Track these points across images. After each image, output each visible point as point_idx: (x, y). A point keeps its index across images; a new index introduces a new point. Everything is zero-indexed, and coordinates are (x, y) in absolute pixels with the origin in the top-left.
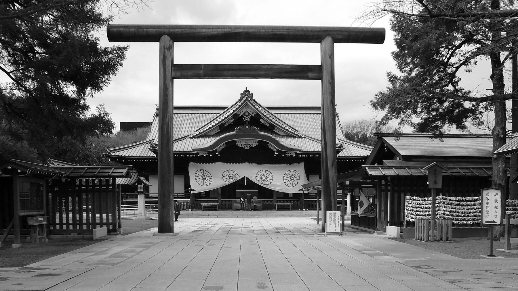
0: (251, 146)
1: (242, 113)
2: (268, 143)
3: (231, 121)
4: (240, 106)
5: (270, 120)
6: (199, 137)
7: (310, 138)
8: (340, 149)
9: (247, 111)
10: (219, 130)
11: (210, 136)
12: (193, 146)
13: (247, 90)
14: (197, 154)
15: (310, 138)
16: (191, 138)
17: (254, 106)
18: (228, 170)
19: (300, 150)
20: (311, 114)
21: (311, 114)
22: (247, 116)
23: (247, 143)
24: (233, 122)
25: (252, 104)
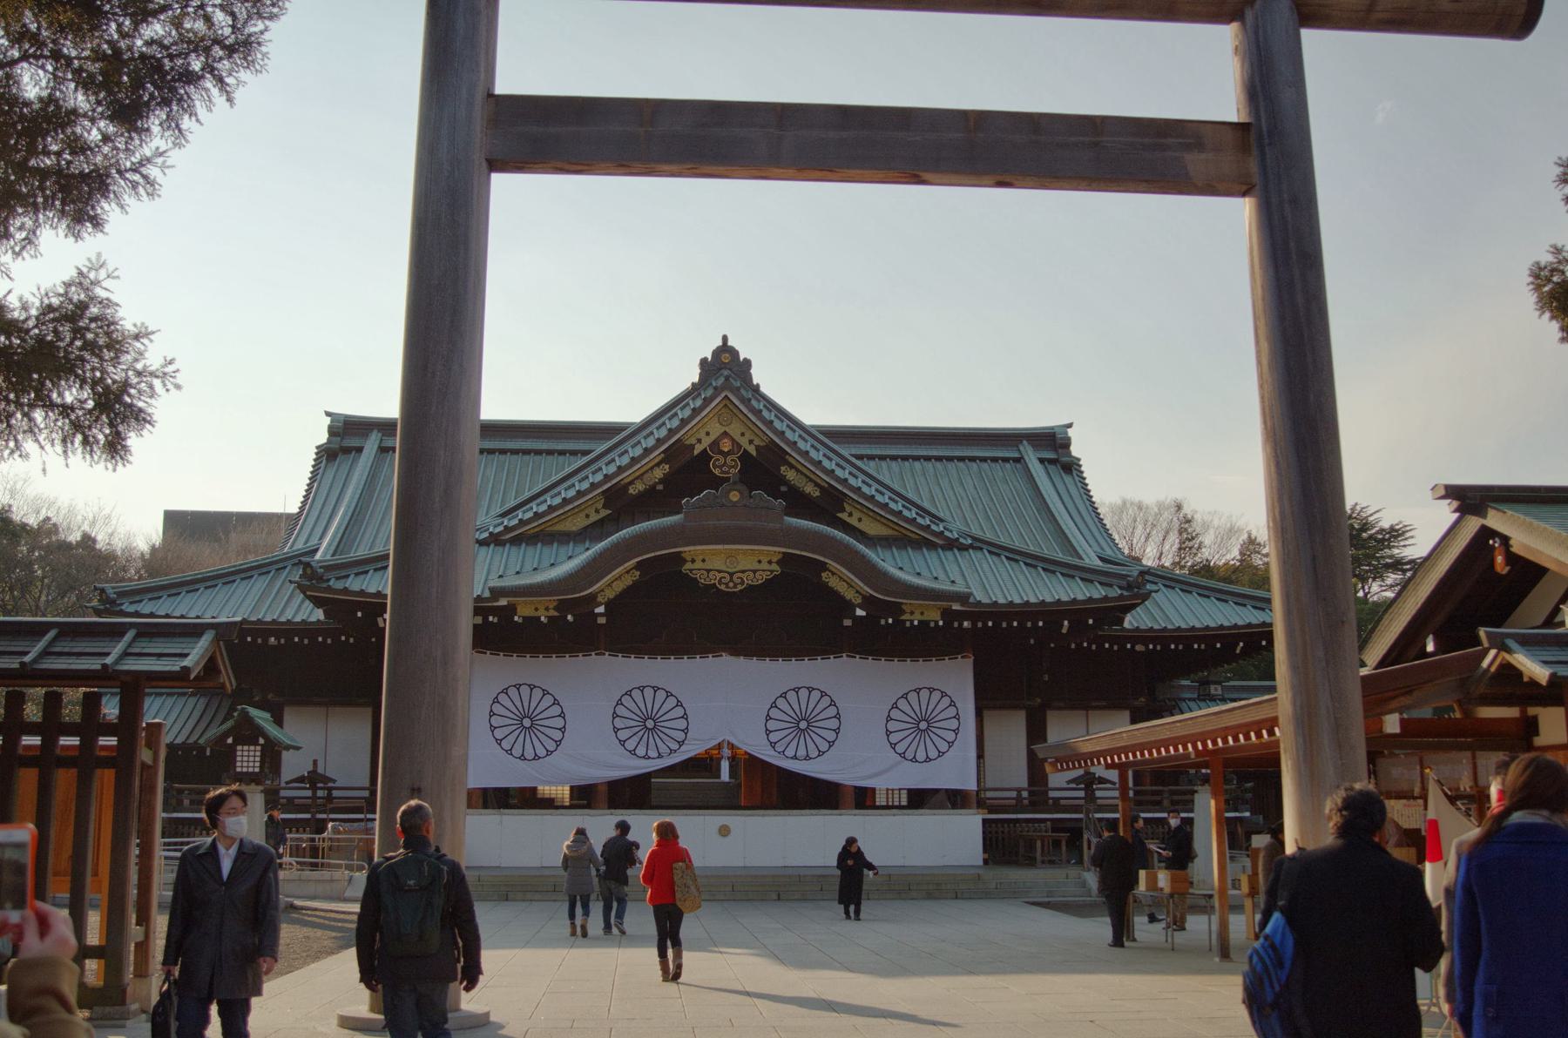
0: (749, 580)
1: (706, 442)
2: (823, 567)
3: (658, 474)
4: (696, 412)
5: (825, 470)
6: (516, 541)
7: (996, 549)
8: (1136, 596)
11: (565, 538)
12: (494, 575)
14: (512, 609)
15: (996, 549)
17: (758, 413)
19: (963, 598)
20: (973, 459)
21: (973, 459)
23: (732, 563)
24: (665, 480)
25: (747, 402)
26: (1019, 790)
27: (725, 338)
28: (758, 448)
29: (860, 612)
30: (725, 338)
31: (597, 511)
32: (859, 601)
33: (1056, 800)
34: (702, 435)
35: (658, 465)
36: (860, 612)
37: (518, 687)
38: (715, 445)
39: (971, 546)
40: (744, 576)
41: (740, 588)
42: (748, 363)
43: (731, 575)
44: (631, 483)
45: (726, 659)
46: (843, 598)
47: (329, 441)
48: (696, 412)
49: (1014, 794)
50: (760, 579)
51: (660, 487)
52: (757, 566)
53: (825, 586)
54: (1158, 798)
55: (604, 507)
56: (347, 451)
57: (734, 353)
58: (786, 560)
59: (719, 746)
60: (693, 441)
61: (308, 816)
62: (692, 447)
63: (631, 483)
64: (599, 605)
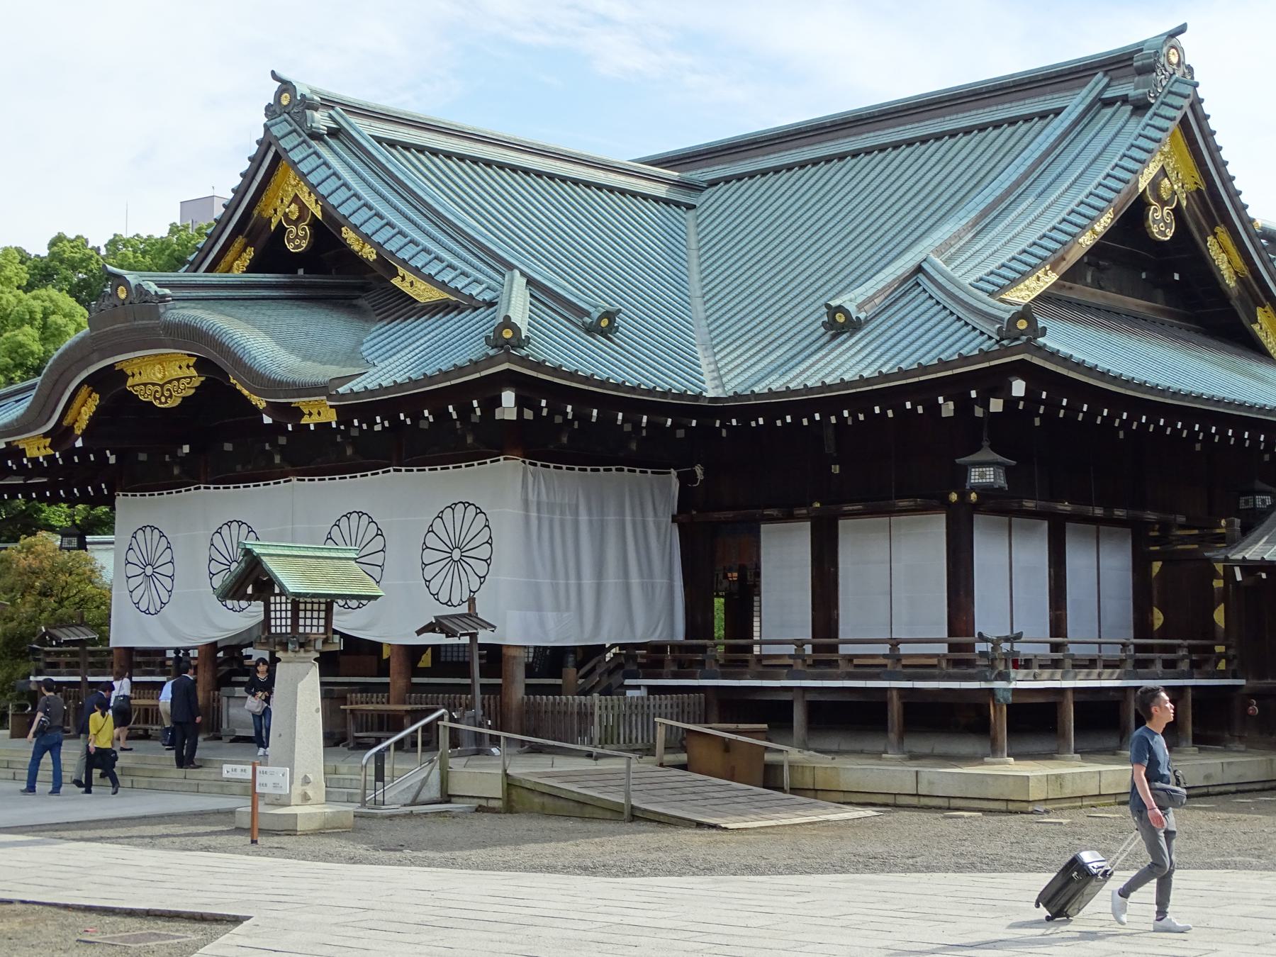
22: (296, 223)
26: (800, 644)
27: (274, 75)
33: (850, 658)
40: (169, 386)
43: (162, 386)
49: (791, 649)
52: (180, 374)
61: (78, 679)
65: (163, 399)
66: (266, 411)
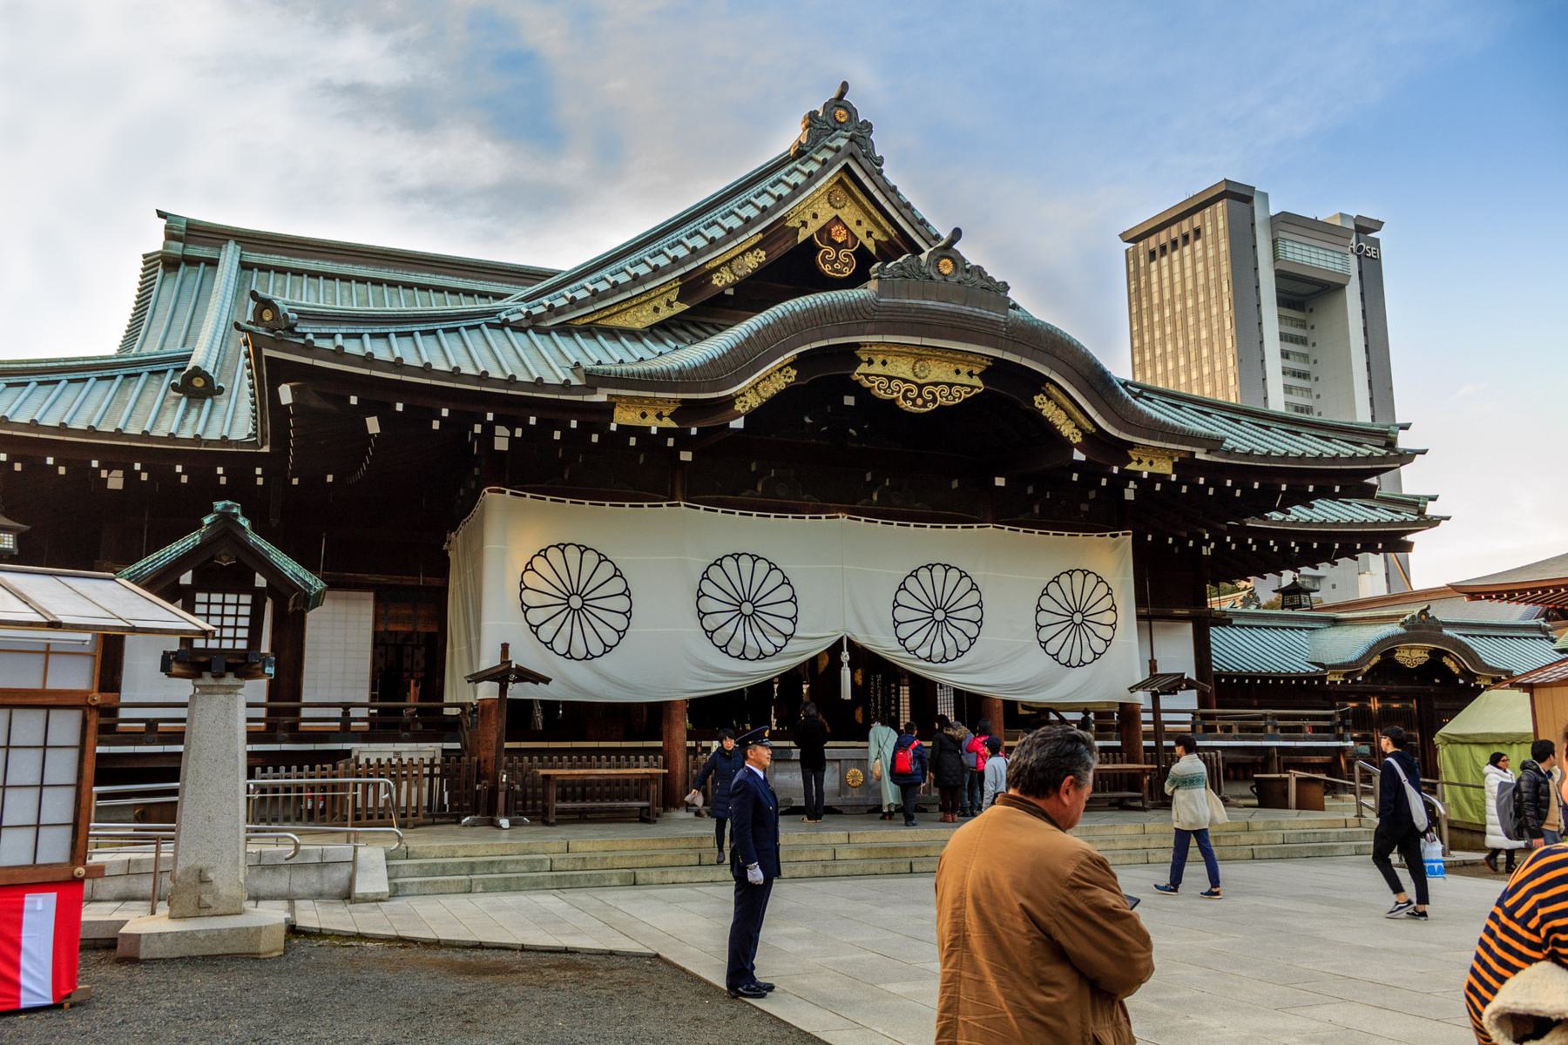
0: (945, 399)
2: (1038, 383)
3: (752, 262)
6: (566, 330)
9: (837, 219)
10: (680, 308)
13: (839, 101)
14: (607, 410)
16: (518, 328)
18: (736, 557)
19: (1213, 444)
22: (838, 247)
23: (917, 376)
27: (845, 86)
28: (877, 243)
29: (1079, 456)
30: (845, 86)
31: (669, 304)
32: (1078, 439)
34: (808, 217)
35: (751, 249)
36: (1079, 456)
37: (562, 547)
38: (824, 231)
39: (1140, 395)
41: (931, 407)
42: (868, 126)
43: (921, 387)
44: (717, 269)
45: (843, 519)
46: (1059, 433)
47: (165, 246)
48: (796, 189)
50: (959, 396)
51: (730, 292)
52: (954, 379)
53: (1037, 416)
54: (1262, 723)
55: (679, 299)
56: (193, 262)
57: (851, 111)
58: (996, 371)
59: (841, 640)
60: (798, 225)
62: (796, 231)
63: (717, 269)
64: (738, 415)
65: (920, 402)
66: (1078, 446)
